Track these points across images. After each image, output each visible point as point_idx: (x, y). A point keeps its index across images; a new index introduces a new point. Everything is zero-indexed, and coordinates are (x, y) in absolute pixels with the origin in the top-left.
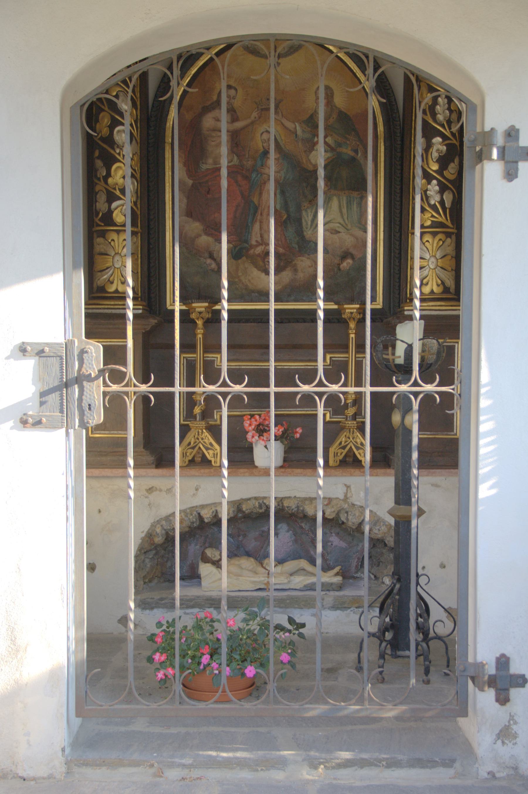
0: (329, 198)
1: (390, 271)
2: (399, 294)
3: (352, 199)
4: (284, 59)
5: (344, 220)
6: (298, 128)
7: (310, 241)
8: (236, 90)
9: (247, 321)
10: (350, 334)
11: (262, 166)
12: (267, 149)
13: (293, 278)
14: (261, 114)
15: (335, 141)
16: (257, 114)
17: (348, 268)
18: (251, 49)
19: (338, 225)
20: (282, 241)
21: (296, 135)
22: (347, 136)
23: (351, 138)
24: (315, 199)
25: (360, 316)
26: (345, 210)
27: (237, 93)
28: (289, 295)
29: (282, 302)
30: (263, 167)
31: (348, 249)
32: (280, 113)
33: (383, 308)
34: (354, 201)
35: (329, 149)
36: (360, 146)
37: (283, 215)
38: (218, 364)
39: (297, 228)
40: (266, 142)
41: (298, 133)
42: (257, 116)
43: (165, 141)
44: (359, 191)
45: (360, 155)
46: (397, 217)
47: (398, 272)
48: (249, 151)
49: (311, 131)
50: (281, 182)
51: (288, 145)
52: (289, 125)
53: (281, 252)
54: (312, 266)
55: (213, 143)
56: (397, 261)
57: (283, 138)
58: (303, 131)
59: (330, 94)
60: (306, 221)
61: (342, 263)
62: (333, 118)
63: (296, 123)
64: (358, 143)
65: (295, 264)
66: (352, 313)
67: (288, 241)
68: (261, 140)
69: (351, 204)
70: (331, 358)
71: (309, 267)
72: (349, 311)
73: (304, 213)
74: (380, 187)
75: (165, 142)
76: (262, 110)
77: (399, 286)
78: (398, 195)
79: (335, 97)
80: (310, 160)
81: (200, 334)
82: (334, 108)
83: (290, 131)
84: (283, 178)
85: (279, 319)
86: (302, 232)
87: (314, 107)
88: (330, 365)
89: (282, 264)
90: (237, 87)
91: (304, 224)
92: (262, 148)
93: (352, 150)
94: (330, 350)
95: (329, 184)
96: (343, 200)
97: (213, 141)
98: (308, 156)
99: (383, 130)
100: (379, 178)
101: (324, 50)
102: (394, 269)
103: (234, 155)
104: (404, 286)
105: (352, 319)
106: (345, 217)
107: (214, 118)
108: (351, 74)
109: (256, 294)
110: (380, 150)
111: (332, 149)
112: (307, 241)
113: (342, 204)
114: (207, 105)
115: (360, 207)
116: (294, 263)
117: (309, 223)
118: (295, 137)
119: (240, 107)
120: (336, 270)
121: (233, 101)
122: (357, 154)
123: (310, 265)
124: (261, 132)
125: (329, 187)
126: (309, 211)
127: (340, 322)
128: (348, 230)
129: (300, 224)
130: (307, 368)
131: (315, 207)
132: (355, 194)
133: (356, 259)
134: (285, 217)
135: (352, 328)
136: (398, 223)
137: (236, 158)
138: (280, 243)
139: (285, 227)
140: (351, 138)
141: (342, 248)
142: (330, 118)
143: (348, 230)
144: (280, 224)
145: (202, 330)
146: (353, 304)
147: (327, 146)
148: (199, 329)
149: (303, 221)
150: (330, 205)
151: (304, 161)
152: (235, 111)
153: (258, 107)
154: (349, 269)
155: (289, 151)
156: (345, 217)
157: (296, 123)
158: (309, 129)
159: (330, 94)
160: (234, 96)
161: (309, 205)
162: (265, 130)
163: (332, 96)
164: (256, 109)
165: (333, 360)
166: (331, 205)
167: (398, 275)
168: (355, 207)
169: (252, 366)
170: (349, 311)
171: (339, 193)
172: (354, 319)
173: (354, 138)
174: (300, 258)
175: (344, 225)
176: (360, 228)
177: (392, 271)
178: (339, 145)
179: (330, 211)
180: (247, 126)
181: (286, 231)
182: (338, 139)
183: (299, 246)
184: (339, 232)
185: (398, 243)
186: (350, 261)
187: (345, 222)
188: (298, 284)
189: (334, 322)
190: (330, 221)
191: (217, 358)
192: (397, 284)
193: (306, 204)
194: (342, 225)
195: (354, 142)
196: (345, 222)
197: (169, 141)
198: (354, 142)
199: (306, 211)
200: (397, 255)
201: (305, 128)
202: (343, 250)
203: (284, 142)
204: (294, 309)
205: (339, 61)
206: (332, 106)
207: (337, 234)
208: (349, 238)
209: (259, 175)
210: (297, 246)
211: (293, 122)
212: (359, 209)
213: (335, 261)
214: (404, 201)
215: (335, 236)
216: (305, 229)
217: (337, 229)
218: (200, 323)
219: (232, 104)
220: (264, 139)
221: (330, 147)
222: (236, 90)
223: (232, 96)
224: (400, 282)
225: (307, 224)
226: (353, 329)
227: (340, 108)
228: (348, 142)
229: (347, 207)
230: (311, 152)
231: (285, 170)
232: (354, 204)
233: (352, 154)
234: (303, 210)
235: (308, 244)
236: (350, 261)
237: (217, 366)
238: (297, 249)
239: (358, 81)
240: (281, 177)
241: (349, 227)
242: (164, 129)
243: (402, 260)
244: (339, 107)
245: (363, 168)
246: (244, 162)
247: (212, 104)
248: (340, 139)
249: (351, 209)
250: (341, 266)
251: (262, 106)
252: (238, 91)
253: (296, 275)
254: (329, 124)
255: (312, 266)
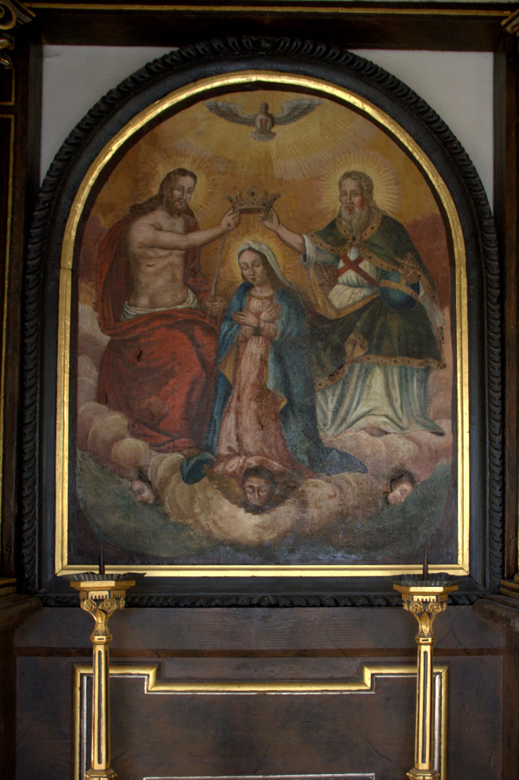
0: (366, 370)
1: (484, 507)
2: (502, 550)
3: (409, 372)
4: (282, 126)
5: (395, 411)
6: (308, 244)
7: (331, 449)
8: (194, 177)
9: (209, 604)
10: (421, 644)
11: (241, 310)
12: (251, 281)
13: (298, 518)
14: (240, 219)
15: (377, 269)
16: (233, 219)
17: (403, 500)
18: (223, 109)
19: (385, 419)
20: (277, 449)
21: (305, 257)
22: (399, 260)
23: (407, 263)
24: (341, 371)
25: (442, 607)
26: (396, 393)
27: (195, 183)
28: (292, 551)
29: (278, 564)
30: (243, 313)
31: (403, 465)
32: (275, 217)
33: (469, 576)
34: (412, 376)
35: (366, 281)
36: (423, 278)
37: (281, 399)
38: (149, 689)
39: (307, 425)
40: (248, 267)
41: (308, 253)
42: (232, 223)
43: (60, 264)
44: (421, 358)
45: (422, 293)
46: (495, 406)
47: (499, 509)
48: (217, 283)
49: (332, 250)
50: (276, 339)
51: (289, 273)
52: (293, 239)
53: (275, 469)
54: (335, 496)
55: (150, 269)
56: (498, 487)
57: (280, 261)
58: (317, 249)
59: (366, 188)
60: (324, 412)
61: (392, 491)
62: (373, 228)
63: (305, 236)
64: (419, 273)
65: (303, 491)
66: (426, 603)
67: (289, 448)
68: (240, 265)
69: (407, 381)
70: (373, 675)
71: (330, 497)
72: (420, 598)
73: (319, 397)
74: (461, 351)
75: (59, 268)
76: (242, 211)
77: (503, 536)
78: (498, 365)
79: (375, 192)
80: (330, 302)
81: (99, 644)
82: (374, 210)
83: (293, 248)
84: (279, 332)
85: (271, 599)
86: (317, 431)
87: (338, 209)
88: (371, 689)
89: (277, 491)
90: (195, 173)
91: (320, 416)
92: (241, 278)
93: (407, 284)
94: (372, 659)
95: (366, 344)
96: (392, 374)
97: (149, 266)
98: (326, 294)
99: (464, 251)
100: (458, 334)
101: (354, 114)
102: (491, 502)
103: (189, 290)
104: (511, 537)
105: (425, 614)
106: (398, 404)
107: (153, 226)
108: (404, 155)
109: (228, 548)
110: (460, 285)
111: (371, 282)
112: (326, 448)
113: (390, 382)
114: (141, 203)
115: (425, 387)
116: (300, 489)
117: (330, 415)
118: (302, 260)
119: (201, 206)
120: (380, 503)
121: (189, 196)
122: (418, 291)
123: (332, 494)
124: (240, 250)
125: (367, 350)
126: (329, 393)
127: (390, 606)
128: (402, 429)
129: (313, 417)
130: (327, 695)
131: (340, 387)
132: (415, 363)
133: (418, 483)
134: (284, 403)
135: (426, 633)
136: (498, 417)
137: (191, 295)
138: (274, 451)
139: (283, 423)
140: (407, 263)
141: (391, 463)
142: (366, 228)
143: (402, 429)
144: (273, 416)
145: (104, 637)
146: (431, 586)
147: (362, 276)
148: (99, 635)
149: (318, 411)
150: (368, 383)
151: (319, 302)
152: (192, 215)
153: (234, 207)
154: (406, 502)
155: (290, 284)
156: (398, 404)
157: (305, 236)
158: (329, 246)
159: (366, 188)
160: (190, 188)
161: (328, 382)
162: (248, 247)
163: (370, 191)
164: (230, 210)
165: (376, 678)
166: (370, 382)
167: (501, 515)
168: (415, 386)
169: (217, 691)
170: (420, 598)
171: (384, 361)
172: (429, 614)
173: (411, 265)
174: (313, 480)
175: (396, 419)
176: (424, 426)
177: (488, 506)
178: (384, 275)
179: (368, 394)
180: (212, 240)
181: (286, 430)
182: (382, 265)
183: (310, 459)
184: (386, 433)
185: (498, 454)
186: (406, 486)
187: (396, 414)
188: (308, 529)
189: (379, 606)
190: (369, 412)
191: (148, 675)
192: (499, 532)
193: (324, 381)
194: (392, 420)
195: (411, 271)
196: (396, 414)
197: (69, 266)
198: (411, 271)
199: (324, 392)
200: (497, 478)
201: (321, 245)
202: (393, 466)
203: (281, 269)
204: (301, 578)
205: (382, 134)
206: (369, 207)
207: (381, 435)
208: (404, 444)
209: (235, 327)
210: (306, 459)
211: (300, 234)
212: (422, 390)
213: (380, 487)
214: (507, 375)
215: (379, 441)
216: (322, 427)
217: (383, 427)
218: (100, 621)
219: (187, 201)
220: (244, 263)
221: (366, 279)
222: (194, 177)
223: (186, 188)
224: (503, 527)
225: (325, 417)
226: (428, 636)
227: (384, 212)
228: (400, 271)
229: (401, 386)
230: (331, 286)
231: (284, 319)
232: (412, 381)
233: (409, 291)
234: (318, 391)
235: (328, 454)
236: (406, 486)
237: (148, 691)
238: (307, 464)
239: (416, 167)
240: (276, 331)
241: (405, 423)
242: (60, 245)
243: (507, 488)
244: (383, 209)
245: (429, 316)
246: (207, 303)
247: (151, 200)
248: (385, 264)
249: (407, 390)
250: (391, 496)
251: (242, 205)
252: (198, 180)
253: (304, 512)
254: (365, 238)
255: (335, 496)
